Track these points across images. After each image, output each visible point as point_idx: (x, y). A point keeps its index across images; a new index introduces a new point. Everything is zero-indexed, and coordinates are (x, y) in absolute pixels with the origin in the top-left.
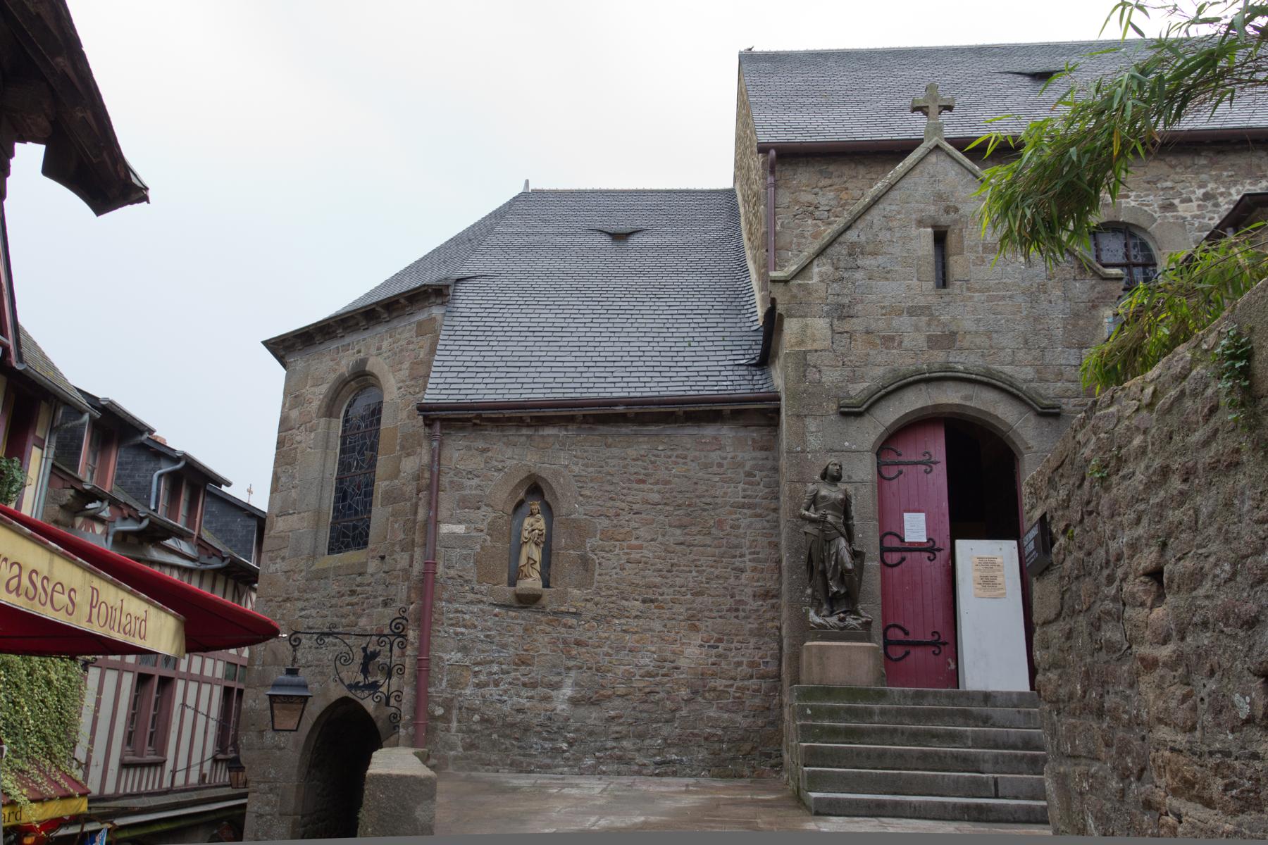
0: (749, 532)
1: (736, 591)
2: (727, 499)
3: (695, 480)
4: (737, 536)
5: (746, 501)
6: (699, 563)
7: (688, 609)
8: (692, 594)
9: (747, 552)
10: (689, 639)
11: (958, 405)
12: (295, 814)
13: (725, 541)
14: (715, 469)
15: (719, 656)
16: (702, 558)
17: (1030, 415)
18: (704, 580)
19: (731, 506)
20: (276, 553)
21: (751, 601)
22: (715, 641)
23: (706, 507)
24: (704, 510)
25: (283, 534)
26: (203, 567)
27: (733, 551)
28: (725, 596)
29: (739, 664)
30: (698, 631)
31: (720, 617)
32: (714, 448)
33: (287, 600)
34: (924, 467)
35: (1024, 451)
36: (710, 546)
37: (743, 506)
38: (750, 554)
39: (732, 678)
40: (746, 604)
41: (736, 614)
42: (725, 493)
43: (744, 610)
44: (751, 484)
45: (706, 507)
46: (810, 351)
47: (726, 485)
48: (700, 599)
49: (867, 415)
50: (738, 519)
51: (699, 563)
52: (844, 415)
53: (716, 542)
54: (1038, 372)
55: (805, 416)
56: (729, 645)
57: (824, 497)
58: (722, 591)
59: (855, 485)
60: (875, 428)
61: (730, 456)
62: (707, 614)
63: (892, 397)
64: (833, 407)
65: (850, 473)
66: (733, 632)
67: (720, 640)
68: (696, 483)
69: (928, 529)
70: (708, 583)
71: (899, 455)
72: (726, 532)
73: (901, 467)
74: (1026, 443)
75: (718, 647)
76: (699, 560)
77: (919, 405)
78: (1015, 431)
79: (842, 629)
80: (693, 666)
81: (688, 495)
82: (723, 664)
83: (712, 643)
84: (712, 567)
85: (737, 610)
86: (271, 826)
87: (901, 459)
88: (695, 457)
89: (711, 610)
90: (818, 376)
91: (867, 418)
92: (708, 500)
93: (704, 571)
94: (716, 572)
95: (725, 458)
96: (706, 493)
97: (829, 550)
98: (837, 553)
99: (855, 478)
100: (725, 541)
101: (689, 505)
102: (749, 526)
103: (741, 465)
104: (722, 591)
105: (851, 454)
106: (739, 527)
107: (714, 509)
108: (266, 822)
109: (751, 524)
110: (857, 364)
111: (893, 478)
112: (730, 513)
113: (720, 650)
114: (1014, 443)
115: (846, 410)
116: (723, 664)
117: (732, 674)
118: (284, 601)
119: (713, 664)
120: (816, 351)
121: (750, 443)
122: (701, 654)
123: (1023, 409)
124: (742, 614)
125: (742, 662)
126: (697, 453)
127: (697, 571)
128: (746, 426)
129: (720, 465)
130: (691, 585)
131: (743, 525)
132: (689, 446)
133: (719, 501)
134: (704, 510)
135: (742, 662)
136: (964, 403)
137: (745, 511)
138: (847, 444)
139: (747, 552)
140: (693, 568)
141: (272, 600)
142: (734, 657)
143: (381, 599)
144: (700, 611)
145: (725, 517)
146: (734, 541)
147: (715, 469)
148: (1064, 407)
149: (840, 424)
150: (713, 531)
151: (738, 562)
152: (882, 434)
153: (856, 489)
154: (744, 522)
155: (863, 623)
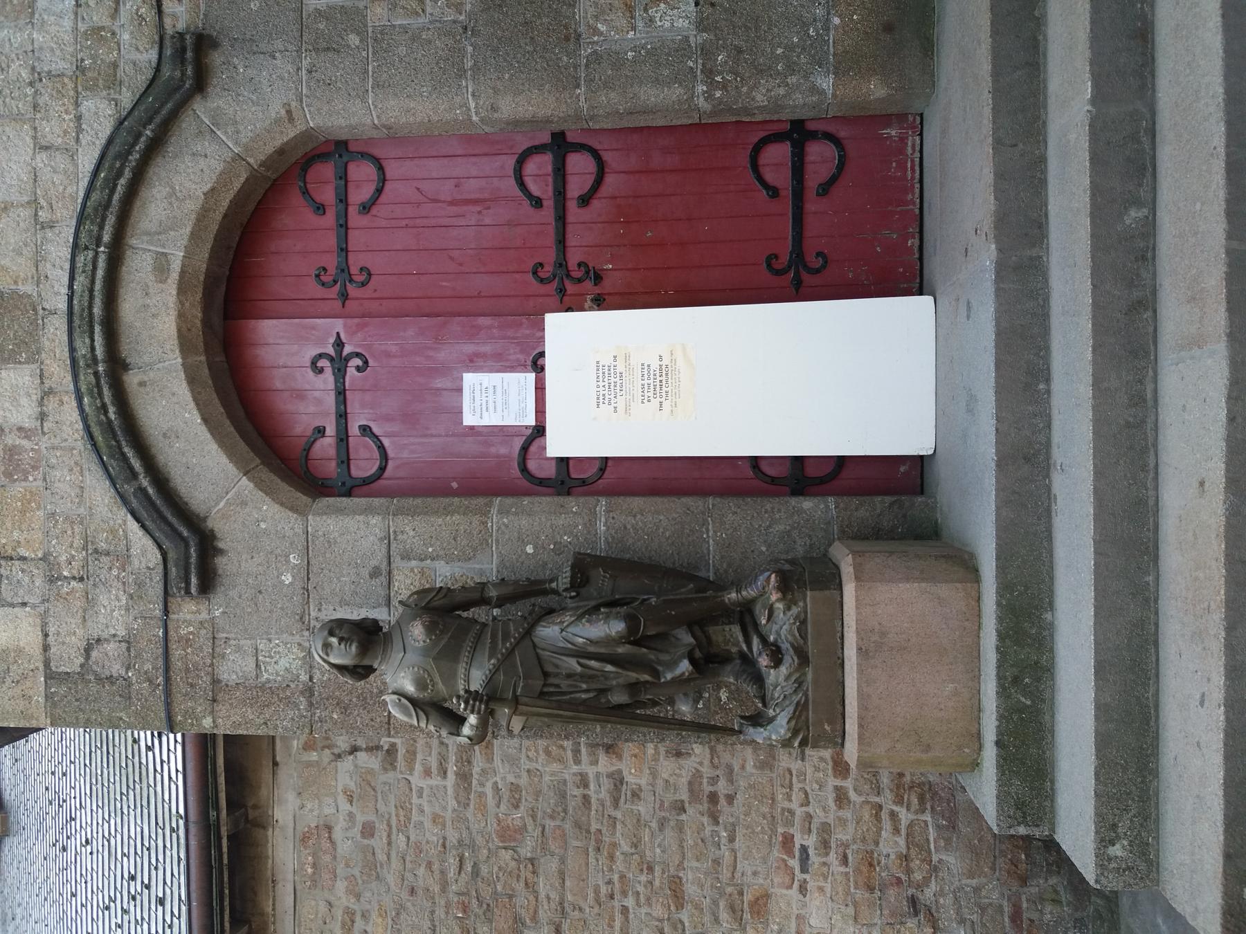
0: (525, 764)
1: (669, 797)
2: (449, 815)
3: (405, 895)
4: (538, 793)
5: (452, 769)
6: (604, 890)
7: (717, 920)
8: (680, 906)
9: (575, 769)
10: (787, 917)
11: (182, 289)
13: (550, 824)
14: (379, 842)
15: (825, 845)
16: (592, 881)
17: (201, 108)
18: (643, 878)
19: (467, 805)
21: (689, 764)
22: (790, 853)
23: (468, 867)
24: (476, 873)
27: (572, 804)
28: (680, 828)
29: (841, 798)
30: (767, 896)
31: (732, 839)
32: (326, 845)
34: (351, 371)
35: (301, 127)
36: (563, 861)
37: (464, 777)
38: (577, 761)
39: (877, 817)
40: (697, 775)
41: (723, 801)
42: (435, 819)
43: (714, 780)
44: (412, 754)
45: (468, 867)
46: (47, 664)
47: (415, 817)
48: (691, 889)
49: (210, 524)
50: (496, 789)
51: (604, 890)
52: (208, 582)
53: (553, 846)
54: (92, 88)
55: (215, 681)
56: (797, 820)
57: (421, 684)
58: (669, 833)
59: (397, 562)
60: (244, 504)
61: (345, 806)
62: (725, 874)
63: (161, 459)
64: (189, 612)
65: (365, 573)
66: (765, 809)
67: (788, 841)
68: (412, 891)
69: (511, 368)
70: (651, 869)
71: (321, 431)
72: (529, 821)
73: (354, 430)
74: (278, 121)
75: (804, 849)
76: (597, 891)
77: (182, 390)
78: (247, 148)
79: (803, 658)
80: (850, 910)
81: (440, 913)
82: (841, 835)
83: (795, 863)
84: (612, 857)
85: (713, 798)
87: (331, 430)
88: (349, 891)
89: (717, 862)
90: (111, 647)
91: (214, 523)
92: (452, 862)
93: (622, 877)
94: (625, 847)
95: (351, 816)
96: (436, 867)
97: (570, 676)
98: (580, 654)
99: (381, 554)
100: (550, 824)
101: (464, 912)
102: (512, 761)
103: (366, 779)
104: (669, 833)
105: (314, 569)
106: (515, 788)
107: (473, 847)
109: (507, 759)
110: (78, 542)
111: (381, 447)
112: (482, 807)
113: (811, 841)
114: (281, 152)
115: (194, 580)
116: (841, 835)
117: (866, 814)
119: (845, 861)
120: (46, 648)
121: (314, 756)
122: (821, 889)
123: (187, 124)
124: (722, 787)
125: (837, 788)
126: (341, 886)
127: (624, 894)
128: (275, 764)
129: (368, 831)
130: (658, 911)
131: (511, 778)
132: (323, 907)
133: (453, 836)
134: (476, 873)
135: (837, 788)
136: (175, 276)
137: (476, 770)
138: (287, 579)
139: (575, 769)
140: (616, 903)
142: (824, 810)
144: (722, 893)
145: (492, 821)
146: (548, 802)
147: (379, 842)
148: (181, 26)
149: (233, 593)
150: (526, 851)
151: (599, 793)
152: (260, 484)
153: (406, 556)
154: (503, 774)
155: (783, 599)
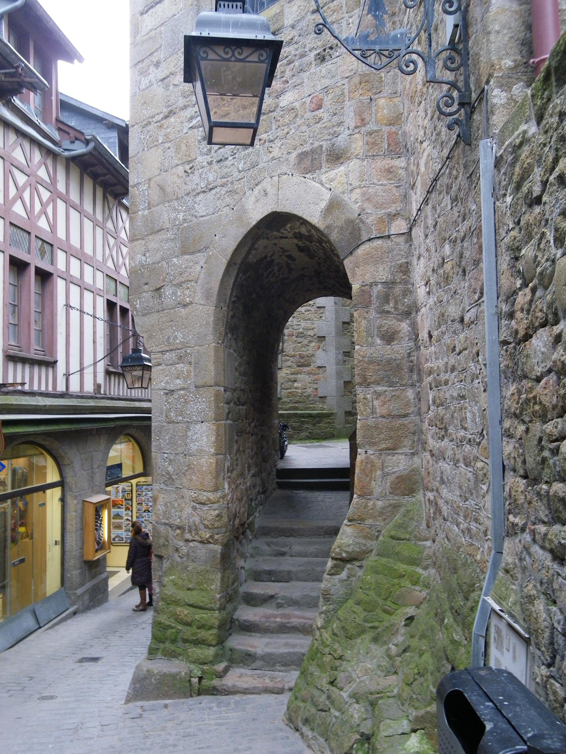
12: (217, 385)
20: (146, 61)
25: (153, 33)
26: (66, 154)
33: (171, 113)
86: (186, 402)
108: (179, 398)
118: (166, 117)
141: (149, 123)
143: (312, 55)
